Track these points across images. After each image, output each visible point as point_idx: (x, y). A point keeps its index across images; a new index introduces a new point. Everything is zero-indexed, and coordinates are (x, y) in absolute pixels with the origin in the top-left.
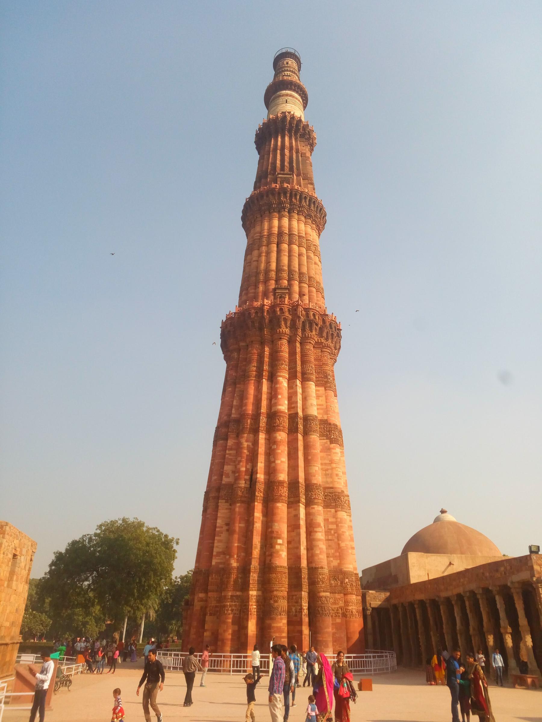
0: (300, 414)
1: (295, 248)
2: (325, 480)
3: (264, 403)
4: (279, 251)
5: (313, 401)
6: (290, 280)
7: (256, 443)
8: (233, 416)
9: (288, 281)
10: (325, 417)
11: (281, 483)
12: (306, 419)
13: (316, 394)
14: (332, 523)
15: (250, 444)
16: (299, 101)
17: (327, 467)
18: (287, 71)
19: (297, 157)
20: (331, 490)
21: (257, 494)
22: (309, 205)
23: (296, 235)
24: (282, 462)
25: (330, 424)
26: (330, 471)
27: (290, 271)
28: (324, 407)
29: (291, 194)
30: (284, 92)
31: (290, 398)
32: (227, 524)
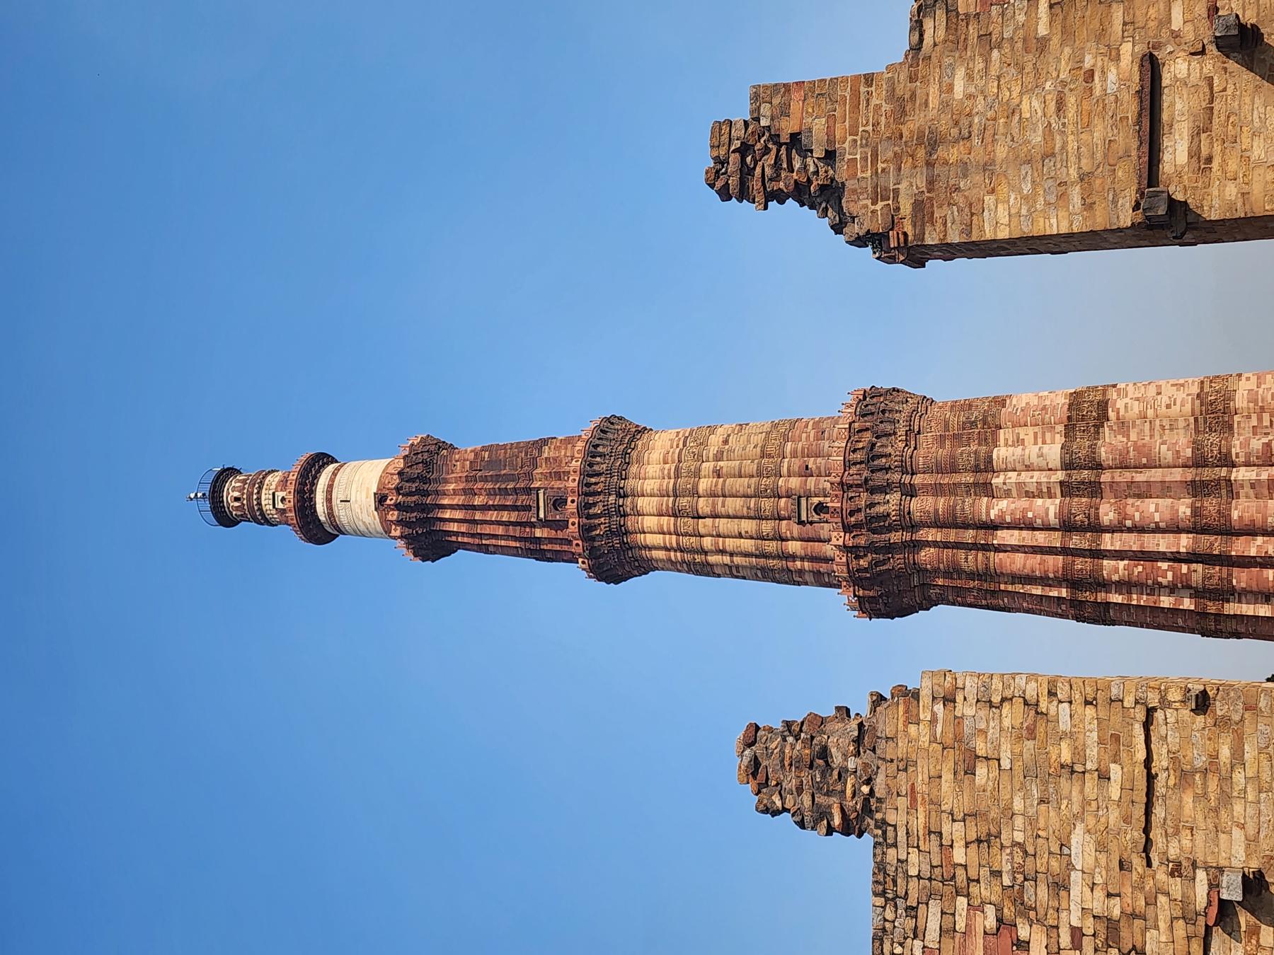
0: (1060, 475)
2: (1182, 432)
3: (1041, 538)
5: (1032, 451)
7: (1119, 555)
8: (1064, 595)
9: (780, 497)
10: (1060, 428)
11: (1196, 512)
12: (1068, 466)
13: (1013, 445)
14: (1260, 419)
15: (1122, 564)
16: (335, 474)
17: (1157, 427)
18: (259, 499)
19: (485, 479)
20: (1201, 420)
21: (1216, 552)
22: (602, 455)
23: (675, 484)
24: (1157, 511)
25: (1069, 418)
26: (1166, 423)
28: (1036, 429)
29: (587, 494)
30: (321, 508)
31: (1029, 495)
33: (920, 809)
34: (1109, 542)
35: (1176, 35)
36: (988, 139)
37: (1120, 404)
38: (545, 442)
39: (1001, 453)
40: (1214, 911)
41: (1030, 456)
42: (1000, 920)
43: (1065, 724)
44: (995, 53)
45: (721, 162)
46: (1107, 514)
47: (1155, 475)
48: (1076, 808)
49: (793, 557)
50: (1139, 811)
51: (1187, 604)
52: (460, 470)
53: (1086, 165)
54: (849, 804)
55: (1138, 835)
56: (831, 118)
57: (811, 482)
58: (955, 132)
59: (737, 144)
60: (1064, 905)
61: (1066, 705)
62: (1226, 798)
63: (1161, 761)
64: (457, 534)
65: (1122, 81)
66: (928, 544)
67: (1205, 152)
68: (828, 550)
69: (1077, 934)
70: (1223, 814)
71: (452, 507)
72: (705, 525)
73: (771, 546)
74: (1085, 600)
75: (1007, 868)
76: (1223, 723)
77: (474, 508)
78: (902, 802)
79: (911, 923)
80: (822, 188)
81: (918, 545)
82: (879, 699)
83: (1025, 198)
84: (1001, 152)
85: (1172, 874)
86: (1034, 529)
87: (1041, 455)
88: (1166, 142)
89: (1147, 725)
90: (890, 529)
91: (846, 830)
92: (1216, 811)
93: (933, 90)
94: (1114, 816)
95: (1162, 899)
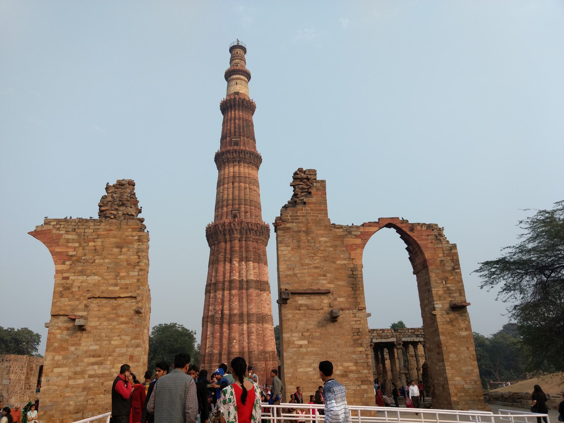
0: (245, 279)
3: (227, 275)
4: (233, 188)
5: (252, 272)
7: (223, 295)
10: (258, 279)
11: (235, 315)
12: (247, 281)
14: (261, 330)
16: (245, 80)
19: (243, 123)
22: (250, 156)
27: (239, 199)
30: (235, 76)
31: (239, 272)
32: (212, 334)
33: (105, 233)
34: (226, 292)
35: (335, 299)
36: (307, 248)
37: (265, 294)
38: (254, 140)
39: (251, 264)
40: (73, 317)
41: (251, 271)
42: (72, 256)
43: (132, 274)
44: (332, 249)
45: (304, 172)
46: (234, 292)
47: (245, 304)
48: (106, 277)
49: (222, 209)
50: (104, 295)
51: (210, 314)
52: (245, 116)
53: (299, 275)
54: (108, 212)
55: (97, 295)
56: (315, 203)
57: (243, 214)
58: (310, 238)
59: (309, 177)
60: (76, 274)
61: (137, 274)
62: (109, 320)
63: (120, 301)
64: (228, 115)
65: (323, 285)
66: (226, 245)
67: (302, 308)
68: (224, 219)
69: (67, 278)
70: (104, 319)
71: (235, 114)
72: (231, 185)
73: (225, 203)
74: (211, 287)
75: (87, 257)
76: (131, 319)
77: (235, 120)
78: (108, 227)
79: (70, 230)
80: (296, 202)
81: (226, 242)
82: (142, 220)
83: (290, 259)
84: (303, 251)
85: (85, 305)
86: (230, 273)
87: (250, 274)
88: (304, 298)
89: (131, 297)
90: (230, 235)
91: (101, 211)
92: (105, 317)
93: (322, 232)
94: (104, 288)
95: (78, 302)
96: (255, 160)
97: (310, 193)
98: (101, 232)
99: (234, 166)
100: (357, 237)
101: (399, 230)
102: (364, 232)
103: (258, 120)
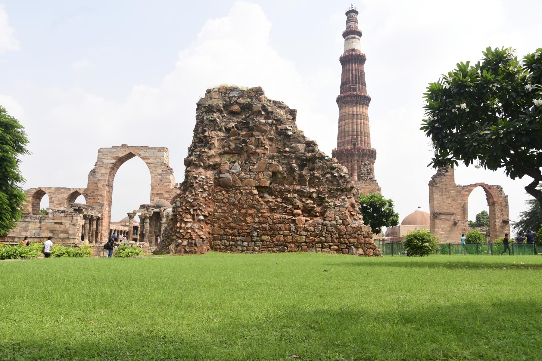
1: (359, 120)
4: (352, 123)
6: (357, 135)
27: (357, 132)
30: (351, 36)
57: (360, 142)
72: (350, 121)
73: (346, 134)
77: (352, 71)
84: (444, 197)
96: (366, 101)
97: (447, 171)
98: (363, 186)
99: (352, 107)
100: (466, 191)
101: (484, 188)
102: (469, 188)
103: (369, 69)
